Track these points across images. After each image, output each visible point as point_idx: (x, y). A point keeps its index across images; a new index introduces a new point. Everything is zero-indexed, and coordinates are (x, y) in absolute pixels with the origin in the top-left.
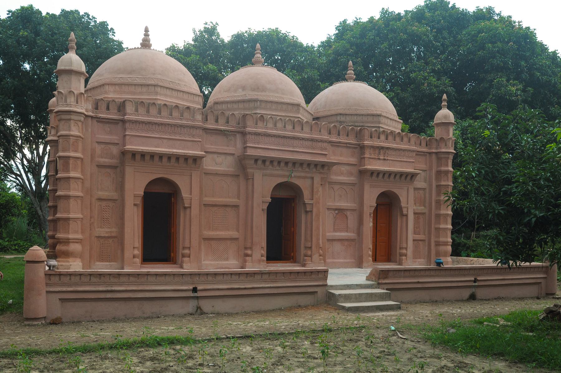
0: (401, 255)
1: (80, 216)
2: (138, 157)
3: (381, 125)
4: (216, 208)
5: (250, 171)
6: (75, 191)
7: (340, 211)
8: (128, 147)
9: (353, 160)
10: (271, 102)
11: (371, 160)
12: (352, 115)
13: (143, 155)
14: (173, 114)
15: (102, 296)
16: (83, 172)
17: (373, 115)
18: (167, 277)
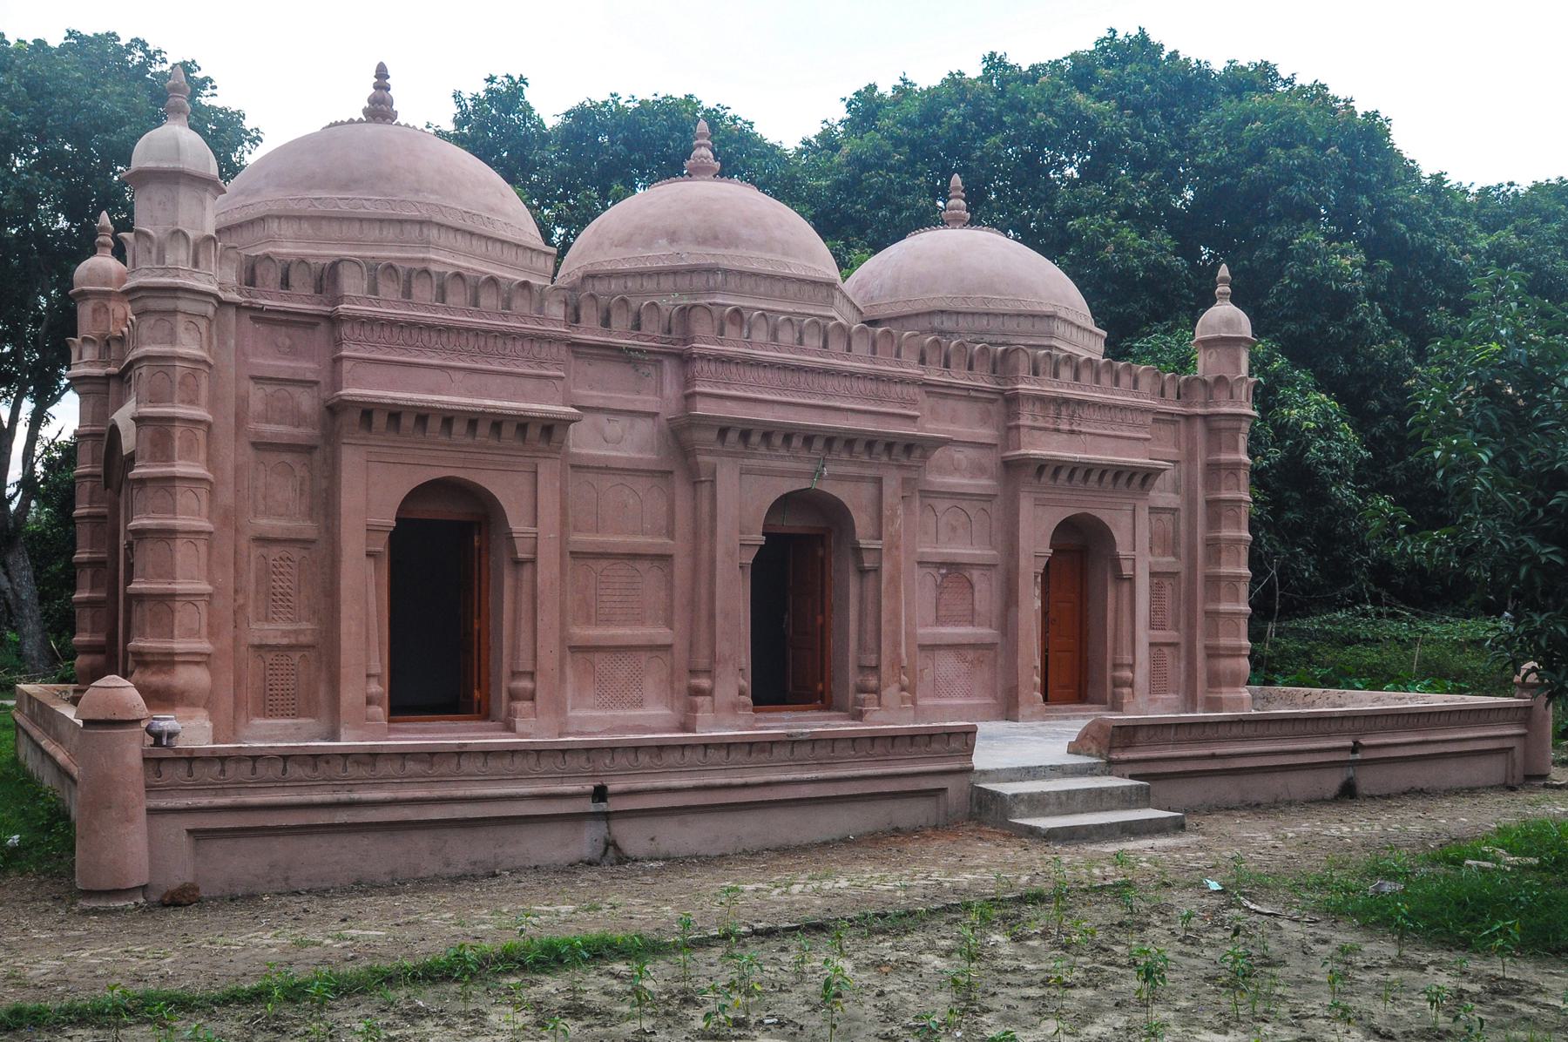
0: (1118, 683)
1: (204, 587)
2: (380, 420)
3: (1054, 343)
4: (604, 563)
5: (703, 459)
6: (190, 515)
7: (954, 569)
8: (350, 391)
9: (985, 433)
12: (973, 314)
13: (395, 414)
14: (482, 301)
15: (323, 818)
16: (210, 462)
17: (1033, 316)
18: (518, 760)
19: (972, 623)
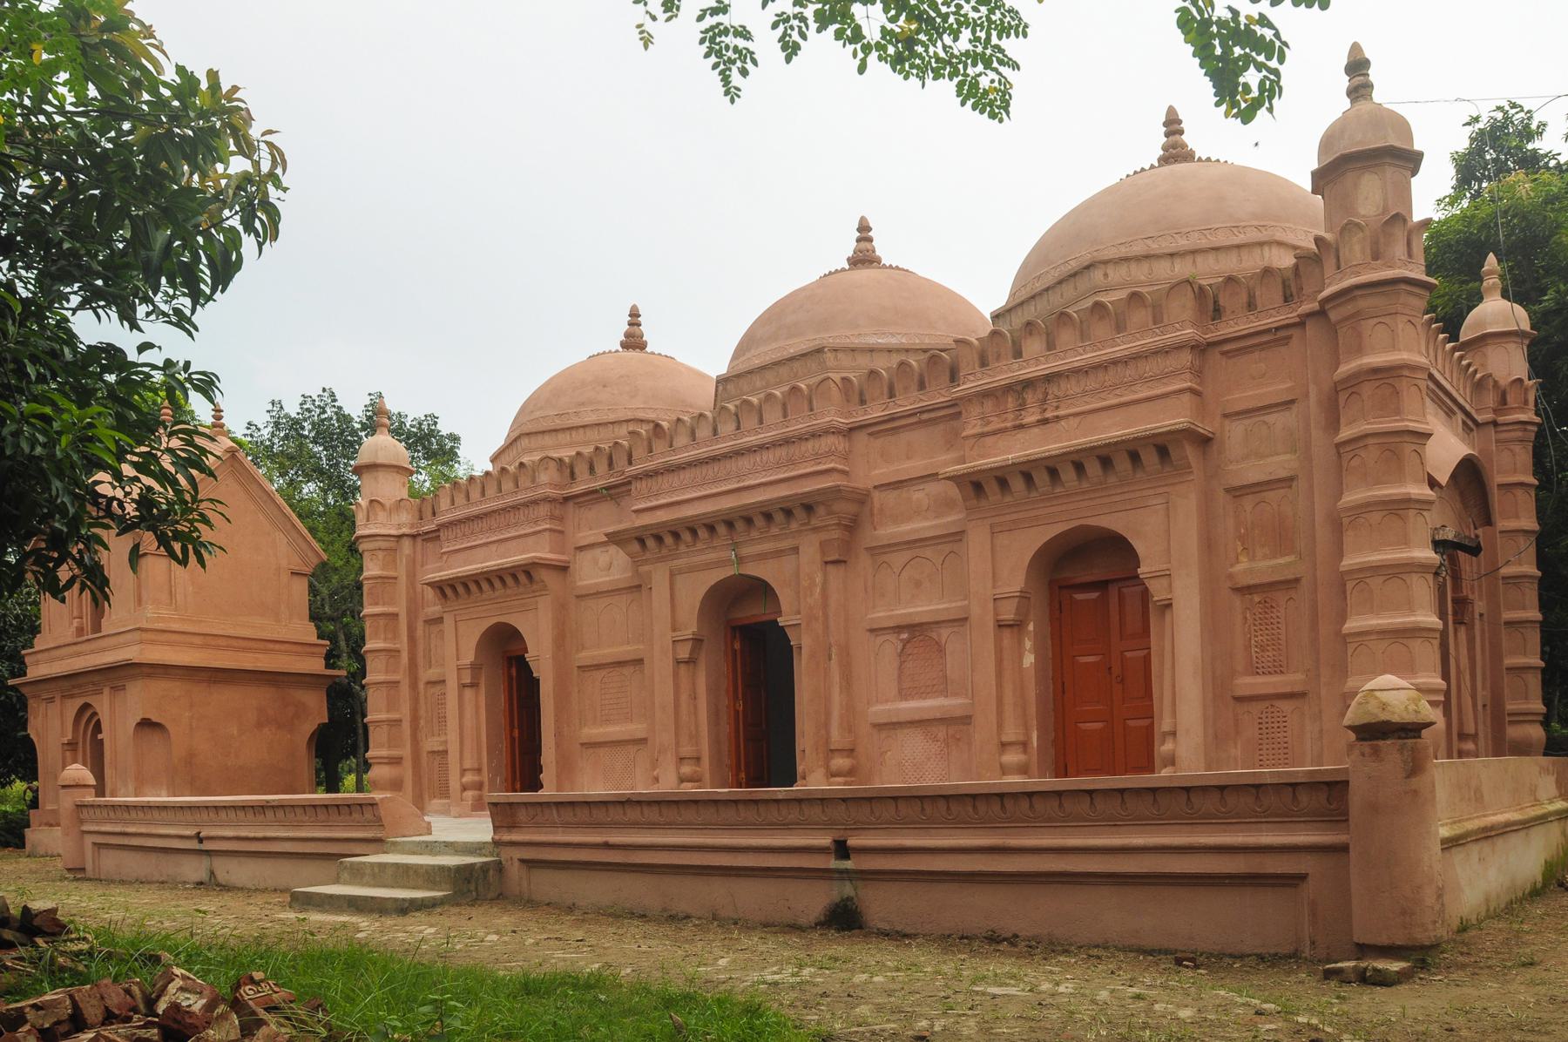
7: (915, 631)
10: (763, 368)
11: (989, 440)
19: (945, 693)
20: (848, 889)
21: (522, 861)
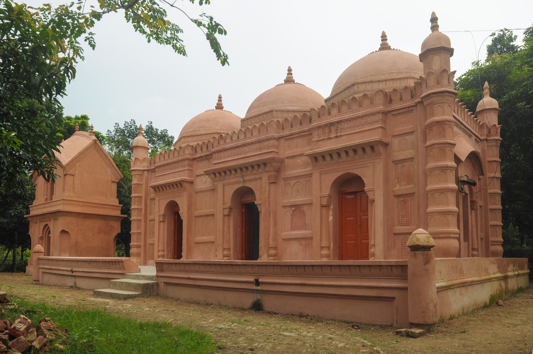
7: (296, 207)
10: (255, 117)
11: (320, 143)
20: (259, 297)
21: (165, 283)
